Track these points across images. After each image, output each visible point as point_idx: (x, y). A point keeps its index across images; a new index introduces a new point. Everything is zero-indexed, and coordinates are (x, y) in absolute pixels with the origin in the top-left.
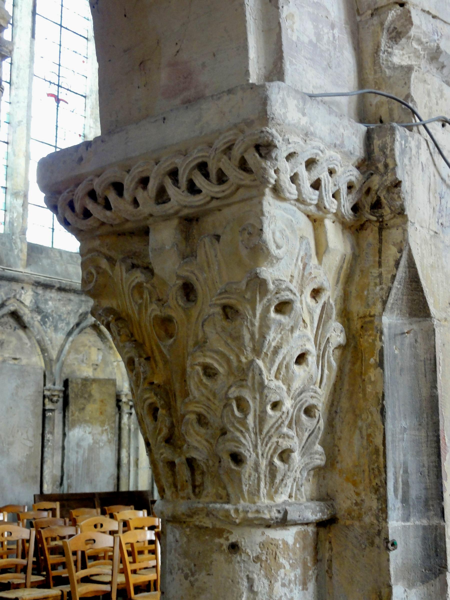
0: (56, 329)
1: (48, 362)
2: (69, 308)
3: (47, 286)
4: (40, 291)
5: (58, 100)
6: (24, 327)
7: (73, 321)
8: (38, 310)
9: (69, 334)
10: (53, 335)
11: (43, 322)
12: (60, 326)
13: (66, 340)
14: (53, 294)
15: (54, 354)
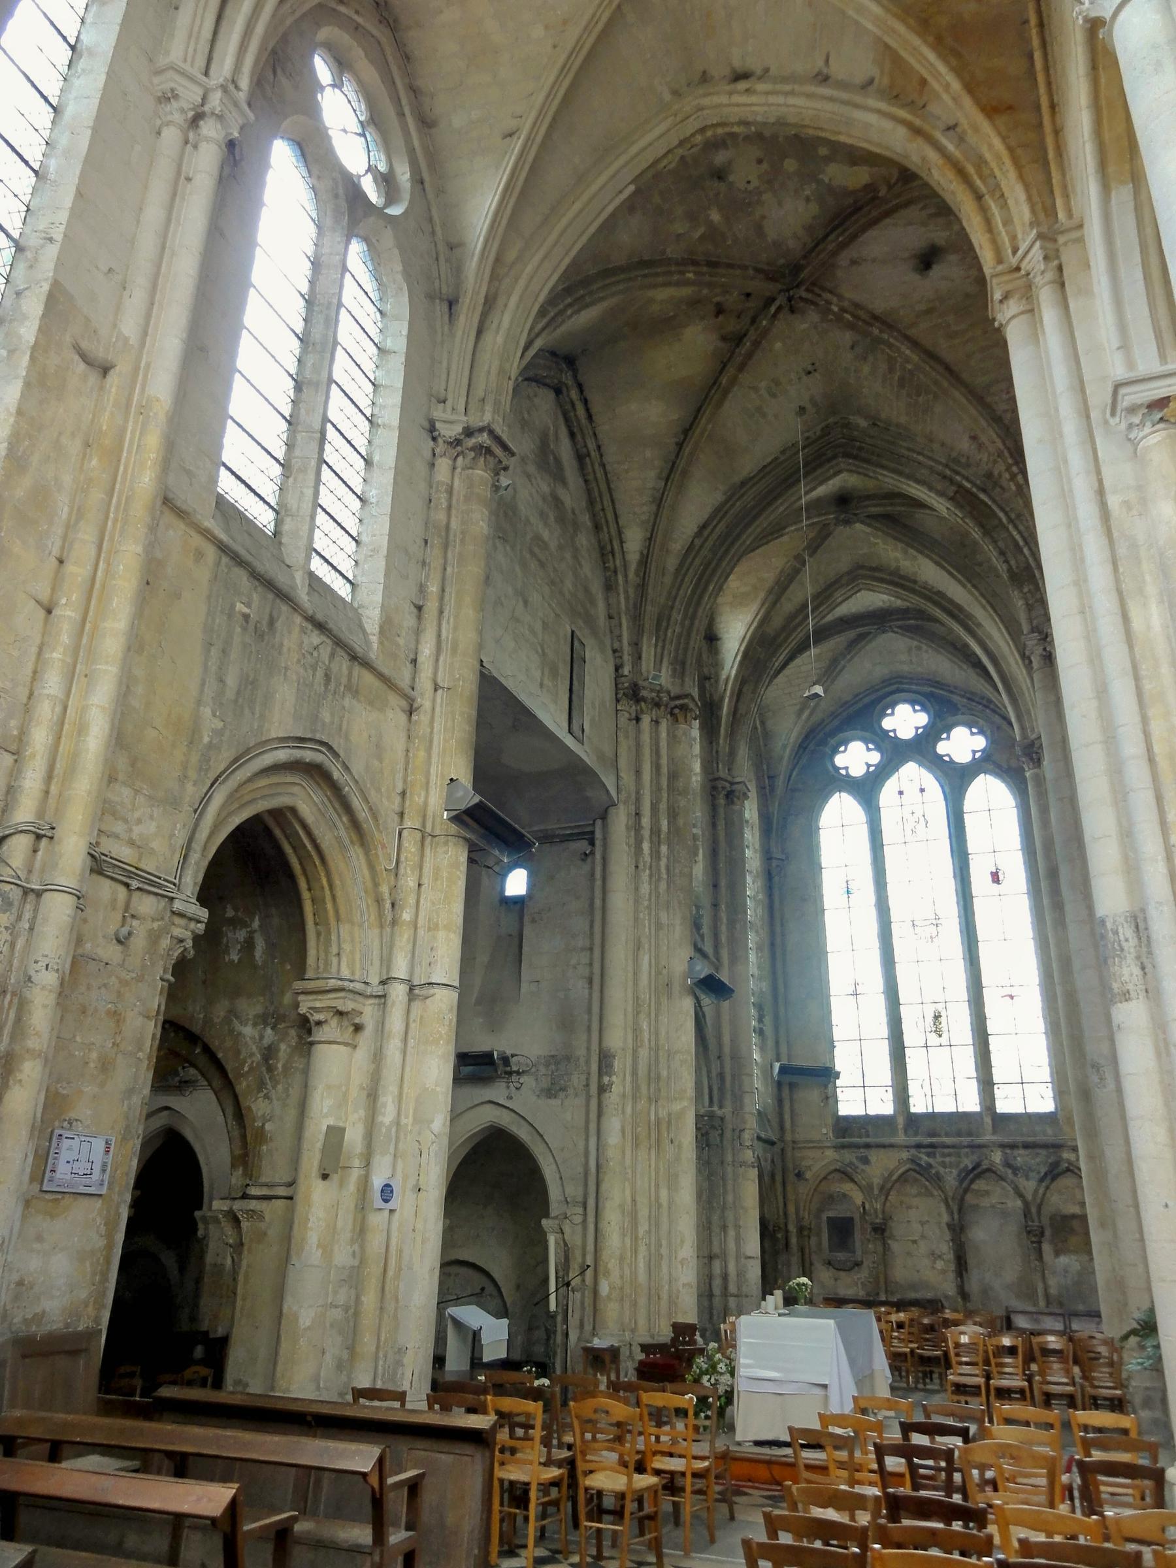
0: (1027, 1178)
1: (1026, 1204)
2: (1038, 1160)
3: (1013, 1146)
4: (1008, 1151)
5: (1012, 997)
6: (1002, 1178)
7: (1043, 1170)
8: (1007, 1164)
9: (1042, 1180)
10: (1025, 1183)
11: (1015, 1175)
12: (1032, 1174)
13: (1039, 1185)
14: (1022, 1151)
15: (1029, 1197)
